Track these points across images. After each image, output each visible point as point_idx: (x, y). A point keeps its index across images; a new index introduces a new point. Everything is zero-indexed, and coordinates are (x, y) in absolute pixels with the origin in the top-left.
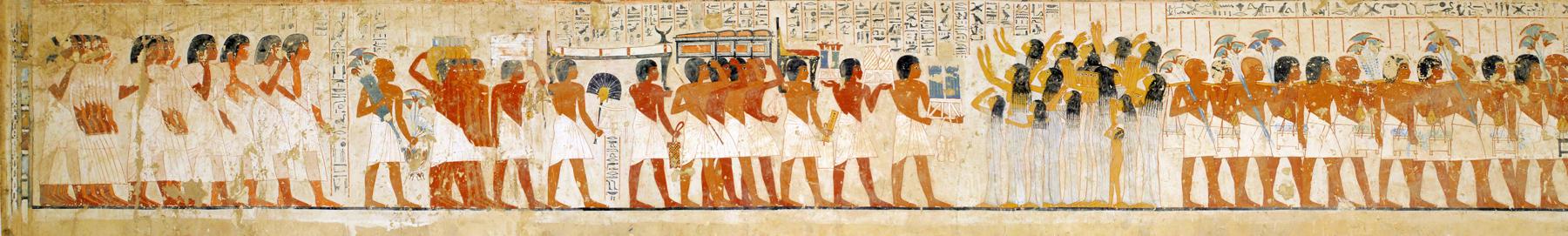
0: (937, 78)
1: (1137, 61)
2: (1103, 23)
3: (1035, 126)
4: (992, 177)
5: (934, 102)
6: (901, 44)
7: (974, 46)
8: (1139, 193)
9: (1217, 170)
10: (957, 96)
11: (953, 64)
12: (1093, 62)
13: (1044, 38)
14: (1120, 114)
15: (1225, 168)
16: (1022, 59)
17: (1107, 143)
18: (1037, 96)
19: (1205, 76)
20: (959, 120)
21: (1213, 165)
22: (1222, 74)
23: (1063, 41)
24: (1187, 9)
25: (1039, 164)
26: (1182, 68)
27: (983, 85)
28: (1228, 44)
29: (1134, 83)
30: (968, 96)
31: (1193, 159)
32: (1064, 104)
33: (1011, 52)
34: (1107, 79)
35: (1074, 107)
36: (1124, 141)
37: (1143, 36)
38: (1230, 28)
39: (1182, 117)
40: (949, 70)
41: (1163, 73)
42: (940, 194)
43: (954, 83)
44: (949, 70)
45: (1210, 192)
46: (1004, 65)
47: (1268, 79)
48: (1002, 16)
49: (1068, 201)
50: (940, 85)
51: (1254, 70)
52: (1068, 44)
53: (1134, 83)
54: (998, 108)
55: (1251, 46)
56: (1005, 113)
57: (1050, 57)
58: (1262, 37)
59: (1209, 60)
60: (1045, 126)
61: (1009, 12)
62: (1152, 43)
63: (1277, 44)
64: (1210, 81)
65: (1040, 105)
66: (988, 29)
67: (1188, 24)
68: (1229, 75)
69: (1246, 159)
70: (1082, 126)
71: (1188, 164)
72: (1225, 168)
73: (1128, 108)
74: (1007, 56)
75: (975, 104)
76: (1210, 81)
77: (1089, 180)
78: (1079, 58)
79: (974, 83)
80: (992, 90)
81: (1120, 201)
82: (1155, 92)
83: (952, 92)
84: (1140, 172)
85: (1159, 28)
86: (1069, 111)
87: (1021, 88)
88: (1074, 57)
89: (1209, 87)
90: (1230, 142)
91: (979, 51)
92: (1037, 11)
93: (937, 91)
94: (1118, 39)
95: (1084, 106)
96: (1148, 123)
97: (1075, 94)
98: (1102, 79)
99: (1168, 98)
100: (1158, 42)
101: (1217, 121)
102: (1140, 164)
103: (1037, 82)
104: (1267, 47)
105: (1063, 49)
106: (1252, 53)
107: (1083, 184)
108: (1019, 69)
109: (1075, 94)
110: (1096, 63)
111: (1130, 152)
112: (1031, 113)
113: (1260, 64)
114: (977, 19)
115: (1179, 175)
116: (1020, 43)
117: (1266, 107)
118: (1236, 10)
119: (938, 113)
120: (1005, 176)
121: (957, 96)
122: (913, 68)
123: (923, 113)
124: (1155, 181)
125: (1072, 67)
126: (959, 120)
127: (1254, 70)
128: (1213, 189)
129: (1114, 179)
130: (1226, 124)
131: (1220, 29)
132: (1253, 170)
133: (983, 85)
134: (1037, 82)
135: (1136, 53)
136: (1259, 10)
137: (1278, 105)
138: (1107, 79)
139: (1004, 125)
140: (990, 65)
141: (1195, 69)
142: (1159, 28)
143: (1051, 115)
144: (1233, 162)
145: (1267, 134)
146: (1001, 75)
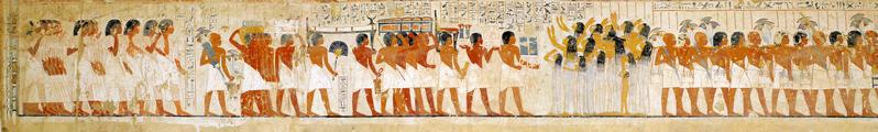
0: (524, 44)
1: (636, 34)
4: (555, 99)
5: (523, 57)
7: (545, 26)
12: (612, 35)
13: (584, 22)
14: (627, 63)
15: (686, 93)
16: (572, 33)
17: (619, 80)
20: (537, 67)
21: (679, 92)
23: (595, 23)
25: (581, 91)
27: (550, 48)
28: (687, 25)
30: (542, 53)
32: (596, 58)
33: (566, 29)
34: (619, 45)
35: (601, 60)
37: (639, 21)
38: (689, 16)
39: (662, 65)
40: (531, 39)
41: (651, 41)
42: (526, 108)
43: (534, 46)
44: (531, 39)
46: (562, 37)
47: (710, 44)
49: (598, 112)
51: (702, 39)
54: (559, 60)
57: (588, 33)
58: (707, 21)
59: (677, 34)
63: (715, 25)
66: (553, 17)
67: (665, 14)
68: (688, 42)
69: (697, 89)
71: (665, 92)
72: (686, 93)
73: (632, 61)
75: (546, 58)
77: (609, 100)
79: (545, 45)
82: (647, 51)
83: (533, 52)
86: (599, 62)
87: (572, 49)
88: (601, 32)
90: (689, 79)
95: (607, 59)
96: (643, 69)
97: (602, 52)
98: (617, 44)
99: (654, 54)
100: (648, 24)
101: (681, 67)
103: (580, 46)
104: (709, 27)
106: (701, 30)
108: (571, 39)
109: (602, 52)
111: (632, 85)
112: (577, 64)
113: (705, 36)
116: (571, 24)
119: (525, 63)
120: (563, 99)
121: (536, 54)
122: (511, 38)
123: (517, 63)
124: (646, 102)
125: (600, 38)
126: (537, 67)
127: (702, 39)
128: (679, 105)
129: (624, 100)
131: (683, 16)
132: (701, 94)
133: (550, 48)
134: (580, 46)
135: (636, 30)
137: (715, 59)
138: (619, 45)
141: (669, 38)
143: (588, 64)
144: (689, 90)
145: (709, 75)
146: (560, 42)
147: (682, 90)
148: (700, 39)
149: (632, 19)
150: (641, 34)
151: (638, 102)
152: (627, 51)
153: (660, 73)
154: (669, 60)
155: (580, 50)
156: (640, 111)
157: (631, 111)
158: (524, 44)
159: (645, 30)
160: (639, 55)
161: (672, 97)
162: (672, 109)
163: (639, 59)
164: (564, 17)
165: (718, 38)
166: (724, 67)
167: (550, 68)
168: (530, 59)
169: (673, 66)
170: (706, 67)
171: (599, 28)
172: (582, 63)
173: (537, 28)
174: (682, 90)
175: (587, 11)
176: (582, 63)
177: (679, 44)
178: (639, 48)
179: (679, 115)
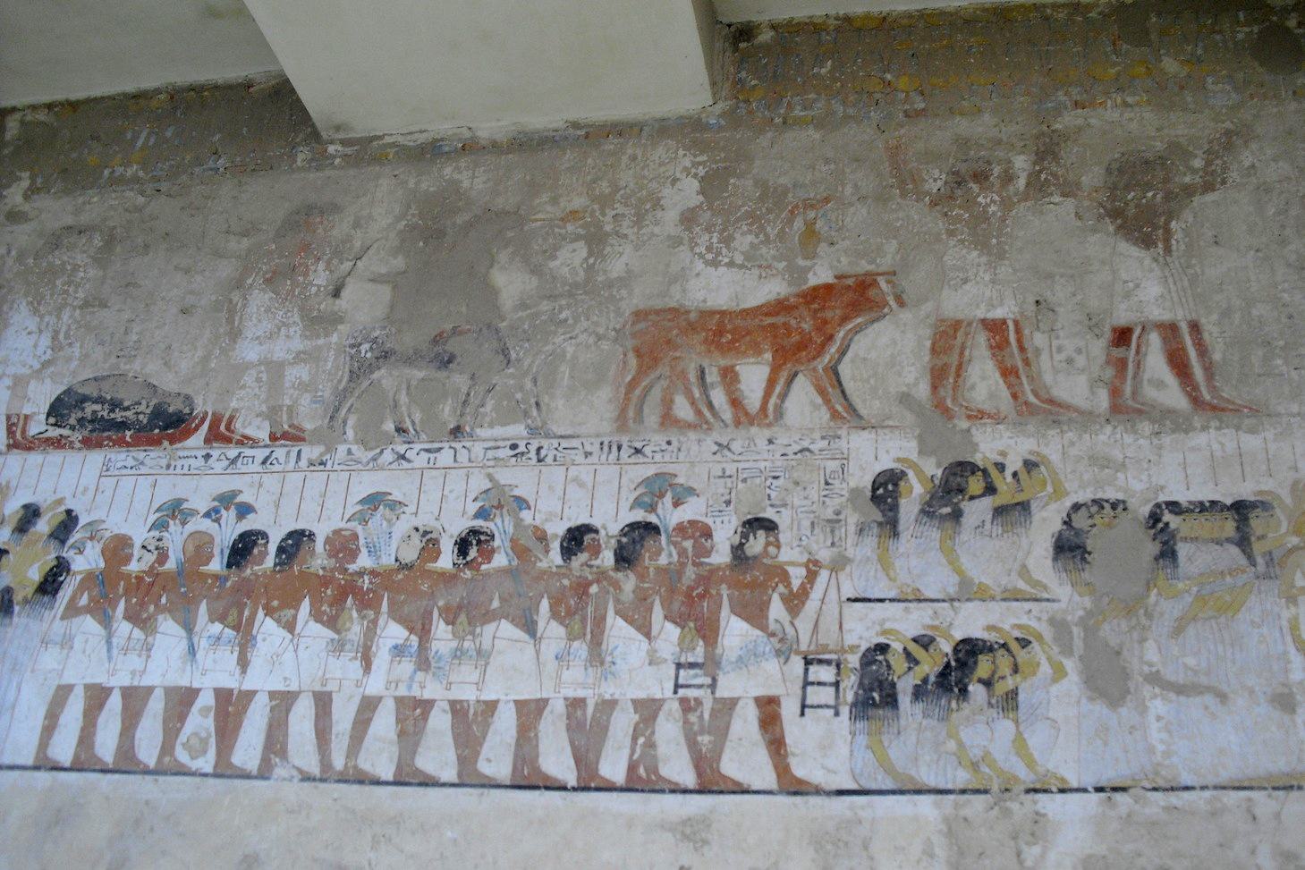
9: (101, 706)
19: (128, 559)
24: (131, 462)
26: (99, 547)
41: (68, 554)
47: (216, 565)
51: (200, 548)
55: (207, 515)
59: (139, 533)
62: (69, 512)
63: (245, 510)
64: (134, 567)
68: (163, 557)
71: (63, 692)
76: (134, 567)
101: (123, 628)
104: (229, 516)
106: (207, 525)
117: (203, 607)
118: (201, 461)
132: (156, 705)
135: (43, 526)
136: (233, 461)
137: (219, 606)
141: (118, 549)
145: (192, 651)
148: (198, 548)
149: (42, 497)
160: (30, 591)
165: (243, 549)
166: (236, 628)
169: (106, 621)
170: (189, 628)
178: (35, 575)
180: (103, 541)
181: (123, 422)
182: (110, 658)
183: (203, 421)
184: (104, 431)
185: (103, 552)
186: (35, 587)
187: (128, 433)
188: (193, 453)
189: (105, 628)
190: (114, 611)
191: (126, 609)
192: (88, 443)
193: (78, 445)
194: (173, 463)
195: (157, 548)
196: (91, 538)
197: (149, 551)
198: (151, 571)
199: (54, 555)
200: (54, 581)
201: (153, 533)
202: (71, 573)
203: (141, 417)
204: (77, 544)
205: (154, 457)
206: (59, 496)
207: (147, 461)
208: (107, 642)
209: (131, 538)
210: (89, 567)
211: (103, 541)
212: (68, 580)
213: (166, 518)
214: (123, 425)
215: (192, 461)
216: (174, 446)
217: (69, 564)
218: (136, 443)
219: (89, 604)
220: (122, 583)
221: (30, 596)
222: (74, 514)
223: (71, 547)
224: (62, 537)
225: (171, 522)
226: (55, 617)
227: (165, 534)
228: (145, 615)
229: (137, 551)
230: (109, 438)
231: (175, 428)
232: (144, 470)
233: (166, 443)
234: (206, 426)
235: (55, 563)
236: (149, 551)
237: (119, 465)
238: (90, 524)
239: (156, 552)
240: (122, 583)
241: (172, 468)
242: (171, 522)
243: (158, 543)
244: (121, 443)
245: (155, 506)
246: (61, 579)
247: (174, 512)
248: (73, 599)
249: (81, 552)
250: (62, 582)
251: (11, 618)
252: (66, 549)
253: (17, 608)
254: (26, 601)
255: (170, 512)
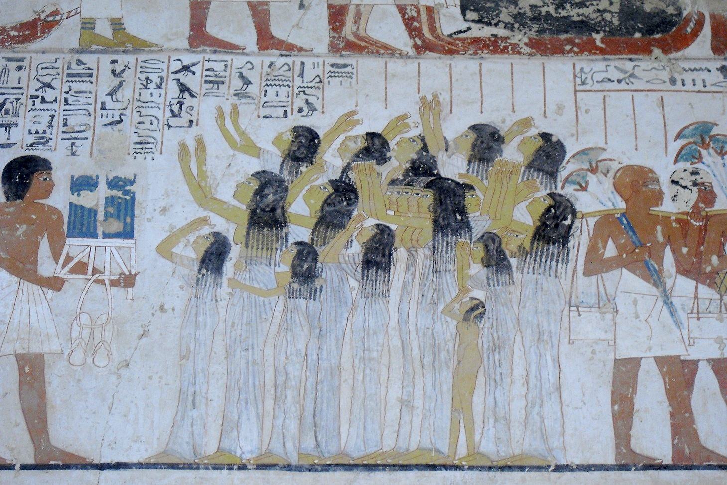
0: (87, 199)
1: (515, 167)
2: (444, 97)
3: (291, 294)
4: (188, 399)
5: (76, 246)
6: (17, 135)
7: (172, 139)
8: (517, 431)
10: (128, 233)
11: (125, 173)
12: (422, 170)
13: (320, 123)
14: (477, 269)
16: (273, 163)
17: (447, 329)
18: (299, 232)
19: (658, 197)
20: (127, 280)
22: (692, 196)
23: (361, 130)
24: (615, 75)
25: (294, 371)
26: (608, 183)
27: (186, 211)
29: (508, 206)
30: (150, 230)
31: (634, 364)
32: (357, 250)
34: (450, 205)
35: (378, 255)
36: (485, 323)
37: (527, 123)
40: (113, 184)
41: (568, 191)
42: (66, 434)
43: (123, 210)
45: (676, 430)
46: (232, 177)
48: (237, 83)
49: (356, 450)
50: (93, 212)
52: (371, 136)
53: (508, 206)
54: (215, 256)
56: (228, 267)
57: (332, 160)
59: (664, 167)
60: (313, 294)
61: (252, 76)
62: (545, 136)
64: (668, 207)
65: (306, 253)
66: (205, 108)
67: (620, 102)
68: (707, 195)
70: (394, 295)
73: (496, 258)
74: (241, 157)
75: (165, 250)
76: (668, 207)
77: (406, 404)
78: (394, 163)
79: (168, 207)
80: (204, 221)
81: (473, 451)
82: (553, 227)
83: (116, 226)
84: (519, 389)
85: (560, 109)
86: (368, 264)
87: (266, 216)
88: (382, 159)
89: (665, 220)
91: (183, 147)
92: (310, 74)
93: (83, 223)
94: (475, 128)
95: (400, 255)
96: (535, 292)
98: (439, 202)
99: (581, 239)
100: (558, 132)
101: (684, 286)
102: (519, 371)
105: (361, 144)
107: (393, 414)
108: (266, 182)
110: (428, 172)
111: (497, 347)
112: (285, 268)
114: (184, 88)
115: (605, 395)
116: (270, 138)
119: (81, 268)
120: (216, 392)
121: (128, 233)
122: (38, 180)
123: (47, 267)
125: (373, 180)
126: (127, 280)
128: (682, 422)
129: (461, 407)
130: (705, 291)
133: (186, 211)
135: (513, 153)
138: (450, 205)
139: (224, 290)
140: (203, 174)
141: (637, 184)
142: (560, 109)
146: (226, 193)
147: (693, 366)
149: (495, 115)
150: (530, 166)
151: (517, 409)
152: (480, 223)
153: (606, 304)
154: (640, 258)
155: (300, 218)
156: (522, 442)
157: (489, 447)
158: (87, 199)
159: (548, 155)
160: (525, 239)
161: (651, 394)
162: (654, 437)
163: (523, 252)
164: (247, 110)
167: (176, 283)
168: (105, 252)
169: (654, 277)
171: (375, 147)
172: (305, 268)
173: (142, 144)
174: (693, 366)
175: (334, 89)
176: (305, 268)
177: (674, 205)
178: (525, 217)
179: (681, 463)
180: (611, 174)
181: (582, 22)
182: (678, 324)
183: (700, 24)
184: (559, 32)
185: (617, 188)
186: (531, 233)
187: (598, 38)
188: (704, 65)
189: (655, 285)
190: (661, 263)
191: (677, 262)
192: (538, 47)
193: (527, 50)
194: (678, 78)
195: (695, 184)
196: (594, 171)
197: (685, 187)
198: (696, 211)
199: (543, 193)
200: (557, 226)
201: (682, 165)
202: (579, 215)
203: (608, 16)
204: (573, 178)
205: (650, 68)
206: (521, 115)
207: (637, 72)
208: (665, 302)
209: (651, 171)
210: (603, 208)
211: (611, 174)
212: (577, 223)
213: (694, 147)
214: (584, 26)
215: (704, 75)
216: (673, 55)
217: (572, 206)
218: (612, 49)
219: (620, 255)
220: (659, 228)
221: (527, 245)
222: (554, 139)
223: (566, 181)
224: (547, 168)
225: (704, 152)
226: (575, 271)
227: (699, 166)
228: (708, 269)
229: (668, 190)
230: (570, 42)
231: (662, 32)
232: (638, 85)
233: (657, 52)
234: (707, 31)
235: (549, 202)
236: (685, 187)
237: (599, 77)
238: (584, 152)
239: (695, 189)
240: (659, 228)
241: (679, 83)
242: (704, 152)
243: (693, 178)
244: (589, 48)
245: (673, 132)
246: (567, 222)
247: (703, 139)
248: (593, 250)
249: (584, 189)
250: (570, 227)
251: (510, 274)
252: (559, 185)
253: (514, 262)
254: (523, 252)
255: (698, 139)
